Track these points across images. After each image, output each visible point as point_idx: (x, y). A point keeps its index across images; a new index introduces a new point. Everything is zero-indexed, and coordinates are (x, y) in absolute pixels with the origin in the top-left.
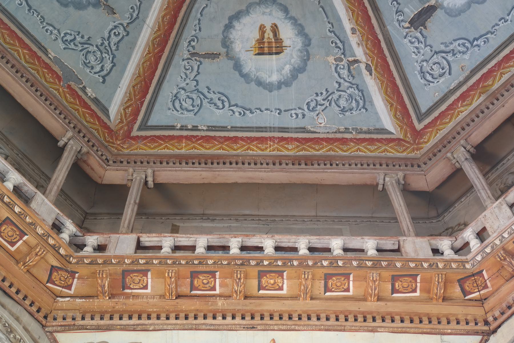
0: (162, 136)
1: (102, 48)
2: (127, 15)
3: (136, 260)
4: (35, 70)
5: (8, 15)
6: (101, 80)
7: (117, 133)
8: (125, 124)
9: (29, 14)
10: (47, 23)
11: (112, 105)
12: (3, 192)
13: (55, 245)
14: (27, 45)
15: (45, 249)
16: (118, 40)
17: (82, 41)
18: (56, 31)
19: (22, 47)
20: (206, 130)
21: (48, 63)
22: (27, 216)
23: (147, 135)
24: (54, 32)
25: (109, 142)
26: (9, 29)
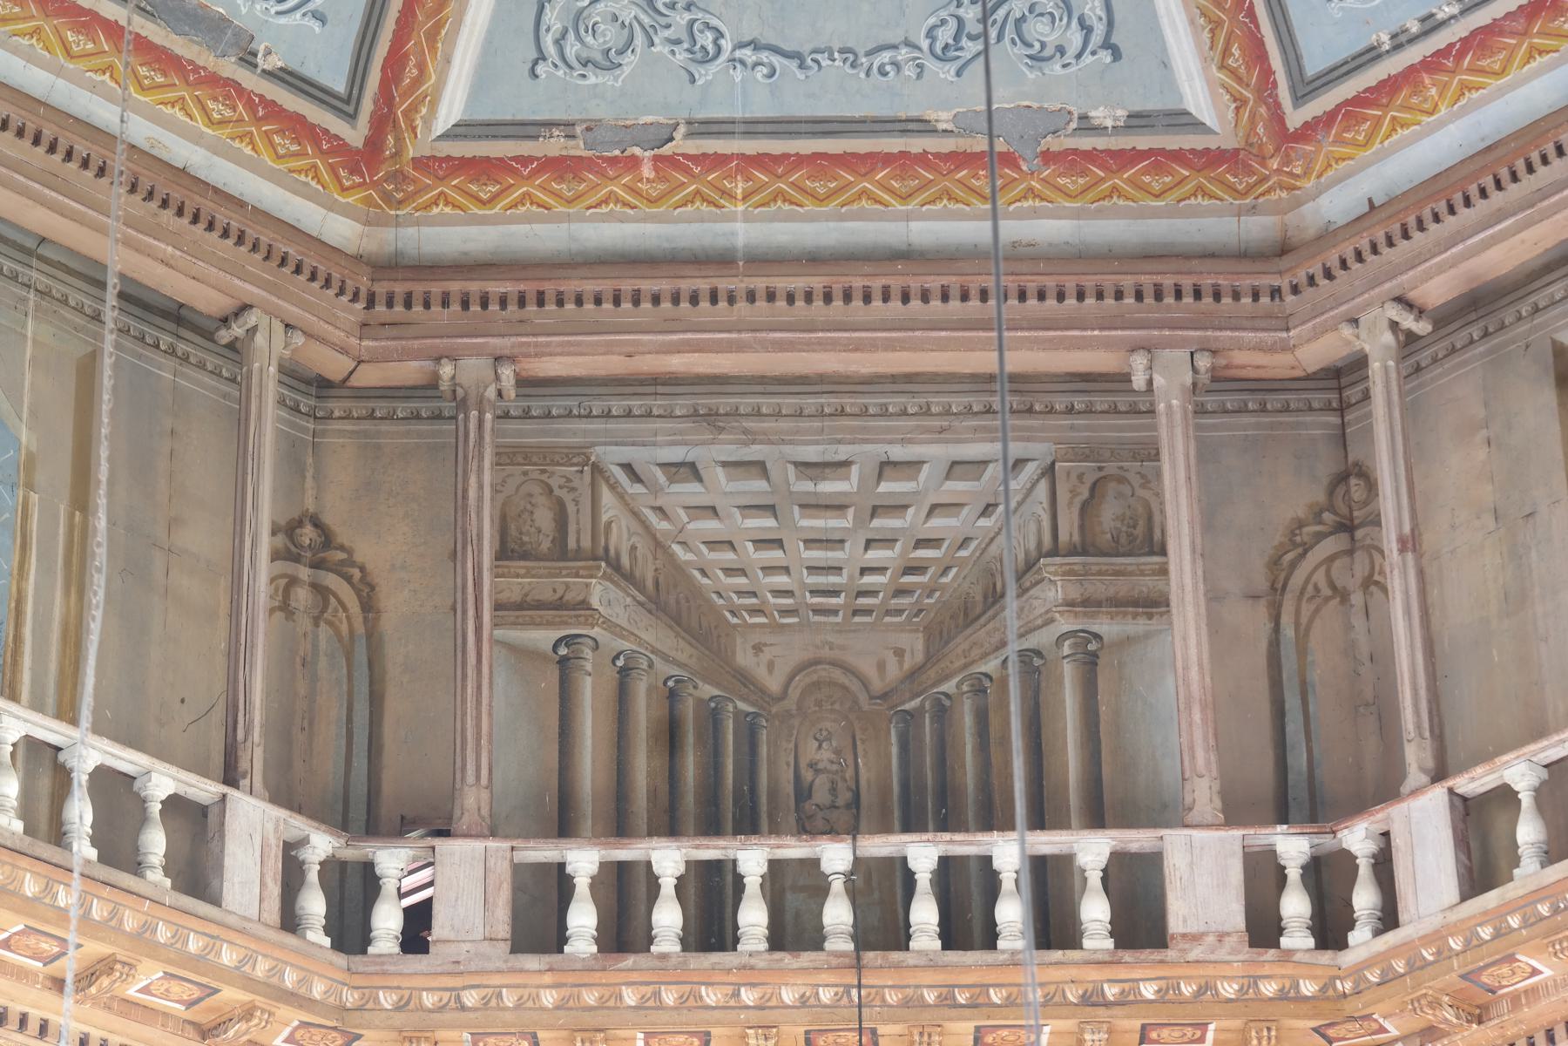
0: (1364, 92)
3: (1472, 933)
5: (769, 128)
6: (1106, 56)
7: (1251, 145)
8: (1255, 101)
9: (810, 73)
10: (868, 54)
11: (1186, 89)
12: (1093, 982)
13: (1284, 987)
14: (870, 156)
15: (1268, 1024)
18: (904, 50)
19: (865, 175)
20: (1462, 13)
22: (1179, 984)
23: (1328, 109)
24: (900, 58)
25: (1250, 188)
26: (800, 160)
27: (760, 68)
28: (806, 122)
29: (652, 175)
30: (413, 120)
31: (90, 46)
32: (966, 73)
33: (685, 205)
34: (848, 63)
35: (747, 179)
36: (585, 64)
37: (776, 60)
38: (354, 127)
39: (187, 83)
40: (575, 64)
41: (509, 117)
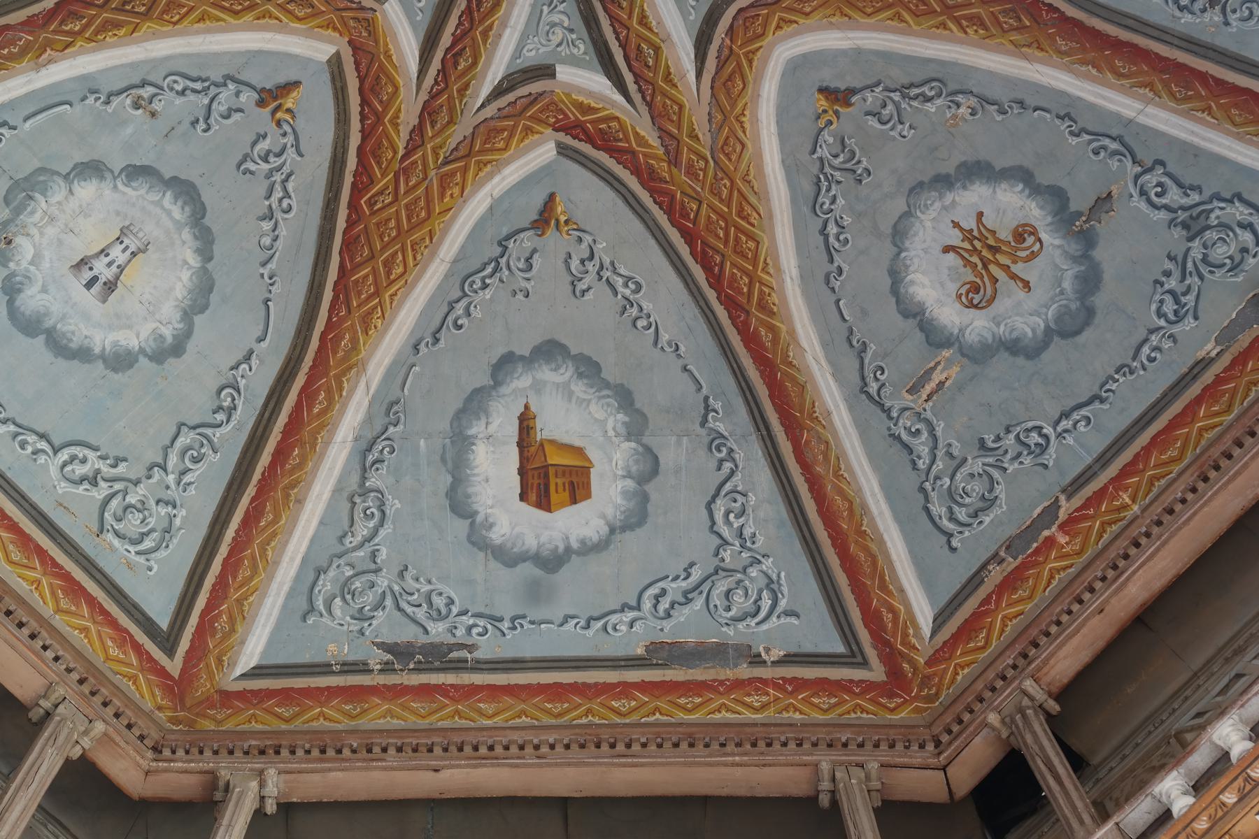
1: (1196, 227)
2: (1114, 164)
4: (1250, 390)
9: (1111, 400)
10: (1134, 359)
16: (1174, 186)
17: (1177, 274)
18: (1153, 337)
21: (1231, 357)
24: (1155, 343)
26: (1147, 449)
27: (1079, 425)
28: (1132, 427)
29: (1067, 539)
30: (910, 643)
31: (633, 703)
32: (1200, 314)
33: (1102, 537)
34: (1128, 374)
35: (1126, 489)
36: (976, 515)
37: (1084, 412)
38: (871, 670)
39: (721, 694)
40: (970, 520)
41: (959, 586)
